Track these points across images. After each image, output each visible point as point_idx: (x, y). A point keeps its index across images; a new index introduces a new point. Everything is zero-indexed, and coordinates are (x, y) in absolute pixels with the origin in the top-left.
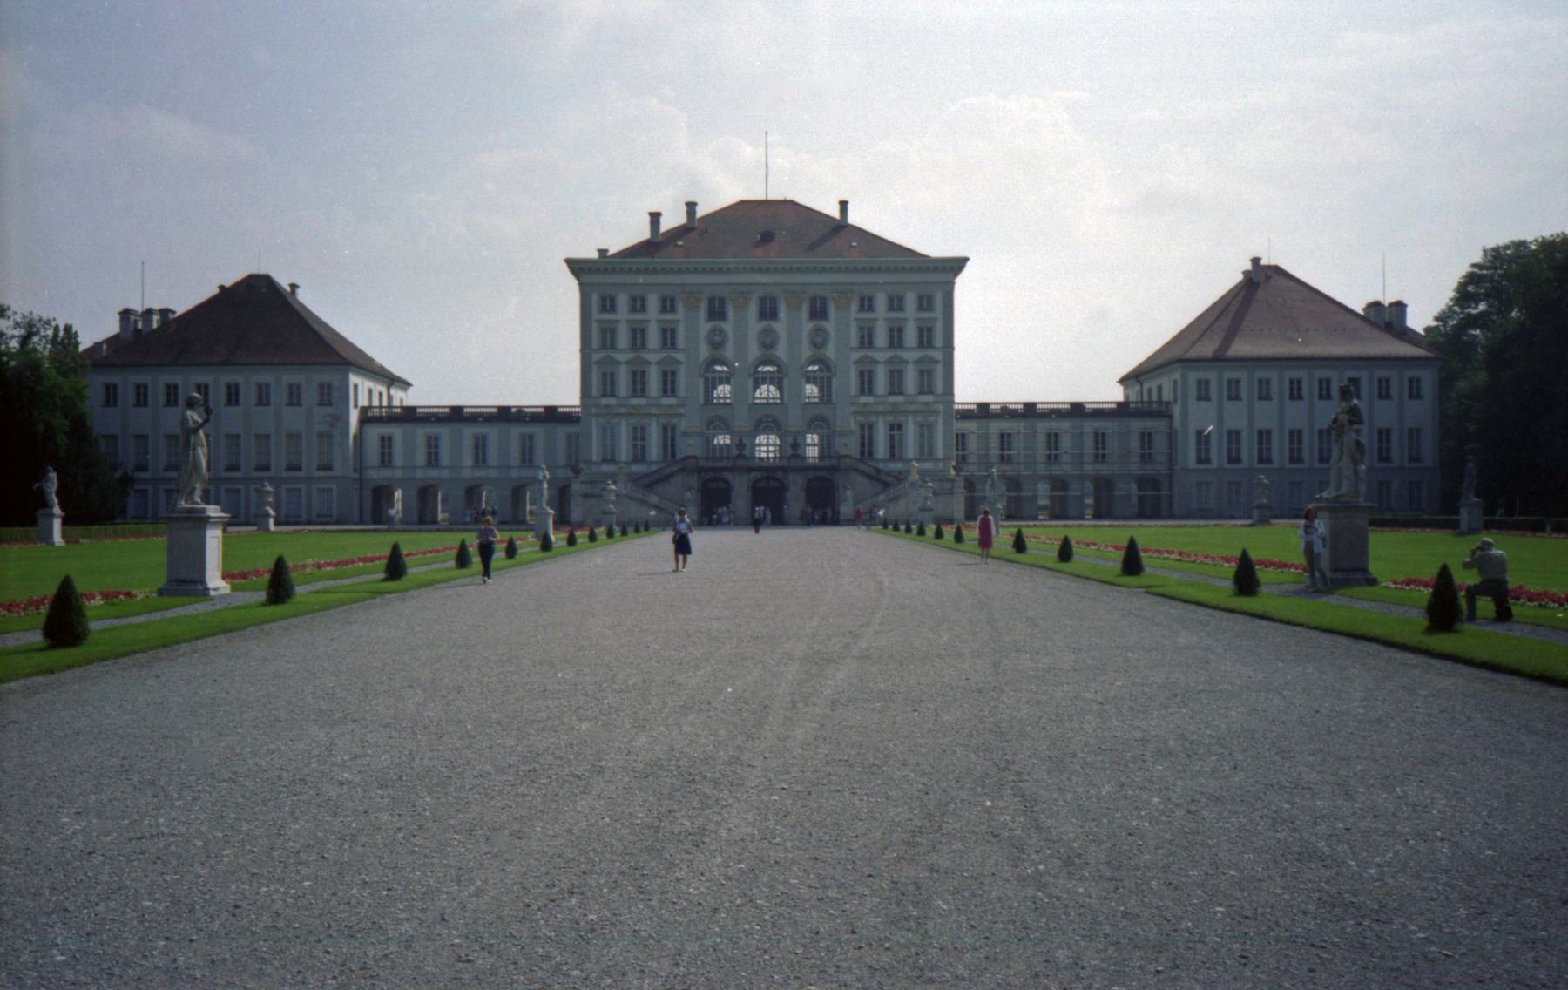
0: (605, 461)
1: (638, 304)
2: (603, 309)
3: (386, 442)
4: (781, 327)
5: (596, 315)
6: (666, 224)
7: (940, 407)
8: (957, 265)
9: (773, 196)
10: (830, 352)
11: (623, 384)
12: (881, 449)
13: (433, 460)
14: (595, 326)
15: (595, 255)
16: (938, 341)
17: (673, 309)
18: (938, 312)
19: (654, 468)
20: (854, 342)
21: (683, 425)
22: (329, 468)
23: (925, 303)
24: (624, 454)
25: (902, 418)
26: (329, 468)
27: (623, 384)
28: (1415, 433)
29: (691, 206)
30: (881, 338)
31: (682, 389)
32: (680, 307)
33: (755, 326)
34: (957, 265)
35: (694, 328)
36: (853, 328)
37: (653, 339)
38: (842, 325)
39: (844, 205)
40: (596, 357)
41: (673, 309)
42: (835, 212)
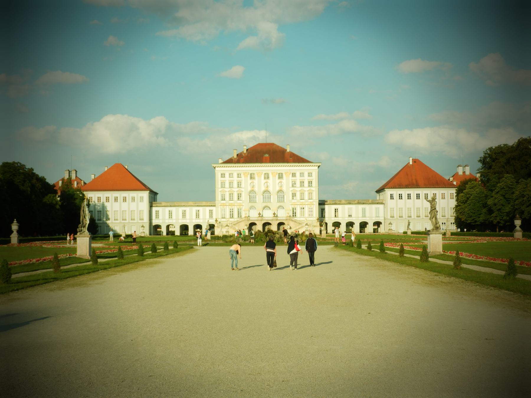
1: (231, 175)
2: (222, 177)
7: (314, 203)
10: (284, 189)
11: (227, 198)
12: (298, 214)
19: (236, 220)
20: (291, 186)
22: (143, 219)
23: (310, 175)
24: (228, 216)
25: (304, 206)
26: (143, 219)
27: (227, 198)
32: (242, 176)
33: (263, 181)
38: (287, 181)
40: (220, 190)
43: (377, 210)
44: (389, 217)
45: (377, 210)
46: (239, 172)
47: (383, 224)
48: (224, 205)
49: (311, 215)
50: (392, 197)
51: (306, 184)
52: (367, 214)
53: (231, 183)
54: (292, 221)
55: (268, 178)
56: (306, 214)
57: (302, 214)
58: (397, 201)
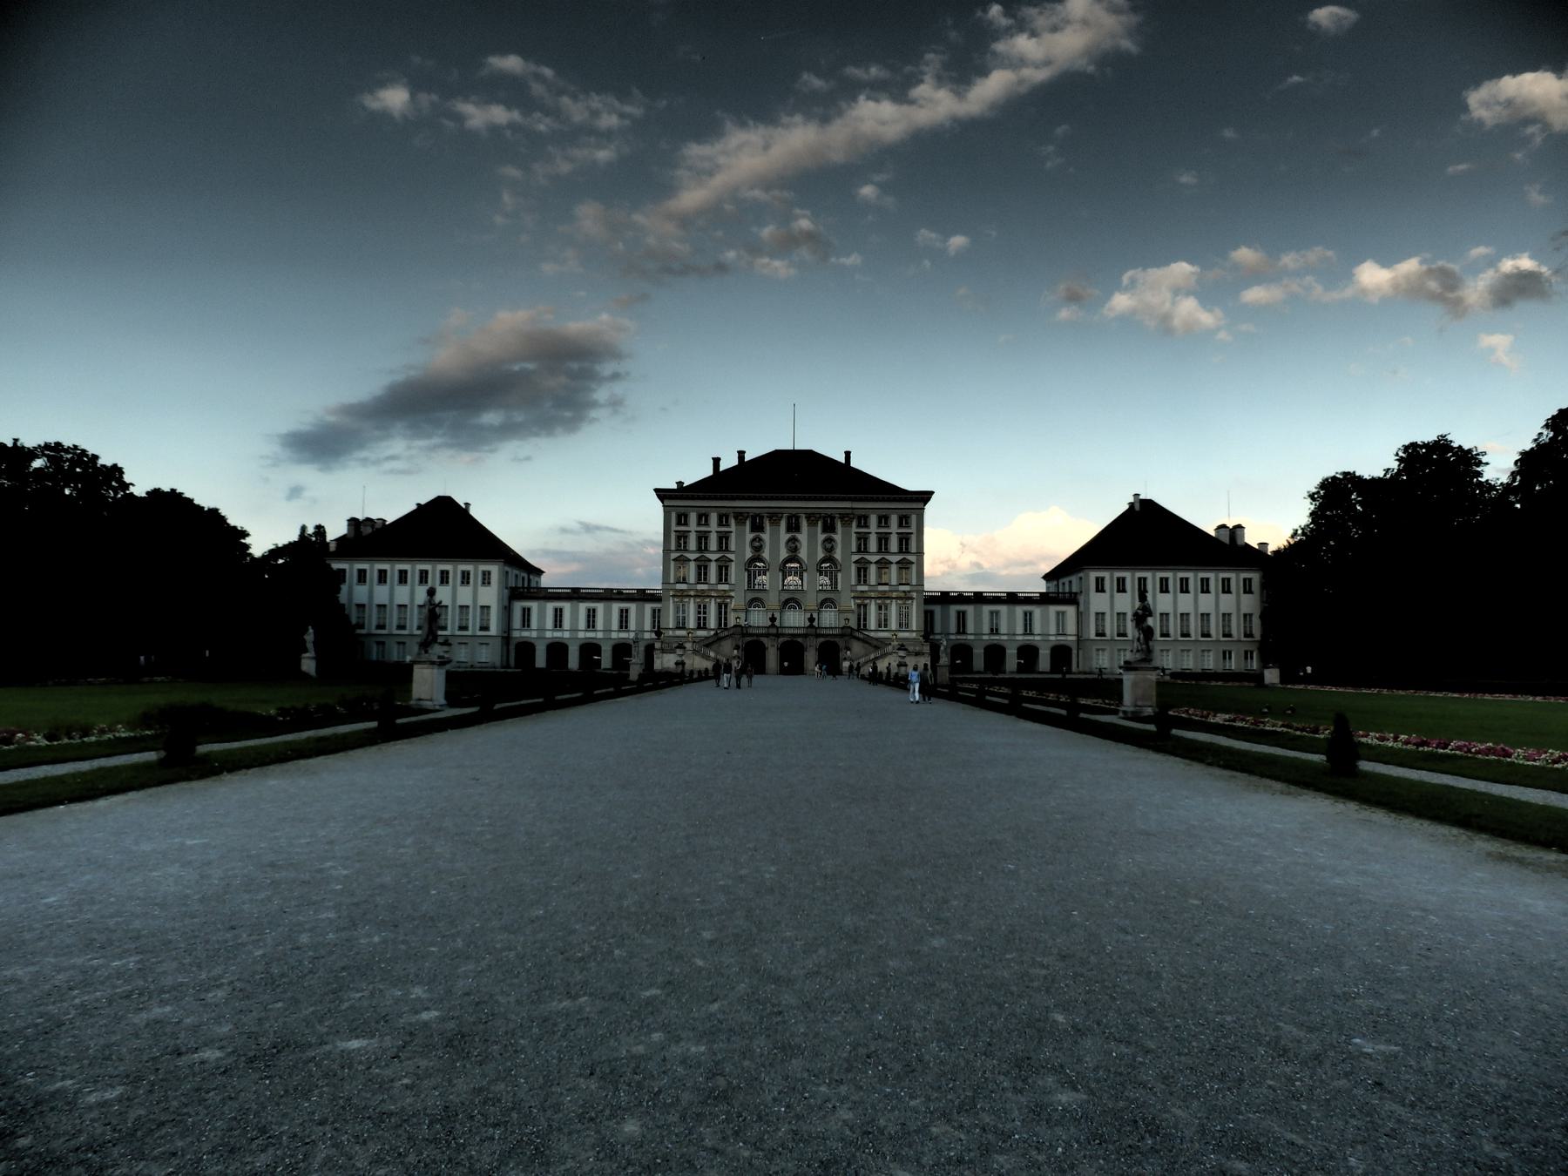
0: (678, 628)
1: (703, 518)
2: (679, 523)
3: (526, 613)
4: (803, 537)
5: (674, 527)
8: (925, 496)
9: (802, 445)
10: (838, 555)
11: (692, 578)
12: (872, 624)
14: (673, 536)
15: (675, 486)
16: (913, 549)
17: (728, 525)
18: (913, 529)
23: (904, 521)
24: (692, 624)
26: (486, 628)
28: (1247, 617)
29: (741, 454)
30: (873, 545)
31: (733, 579)
32: (732, 522)
33: (784, 536)
36: (854, 537)
39: (848, 454)
40: (674, 555)
41: (728, 525)
42: (843, 460)
43: (1061, 616)
44: (1093, 636)
45: (1061, 616)
46: (724, 511)
47: (1074, 652)
48: (682, 595)
49: (904, 624)
50: (1100, 588)
51: (894, 545)
52: (1037, 628)
53: (703, 538)
54: (858, 639)
55: (798, 529)
56: (893, 625)
57: (883, 623)
58: (1112, 597)
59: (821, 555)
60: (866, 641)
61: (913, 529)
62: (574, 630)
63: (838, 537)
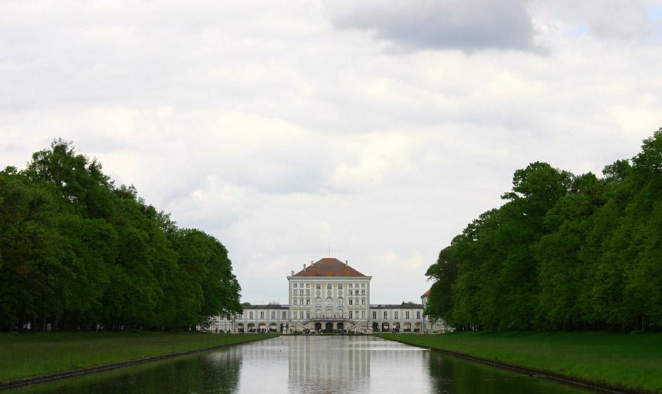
4: (332, 291)
5: (292, 288)
6: (306, 267)
9: (331, 257)
10: (343, 296)
11: (298, 303)
13: (251, 318)
14: (292, 291)
16: (366, 293)
21: (311, 311)
24: (299, 317)
27: (298, 303)
33: (327, 290)
34: (370, 278)
35: (313, 290)
37: (305, 293)
38: (345, 290)
51: (360, 293)
53: (302, 291)
55: (331, 288)
56: (360, 317)
59: (338, 296)
60: (352, 323)
61: (366, 288)
62: (256, 319)
63: (343, 290)
